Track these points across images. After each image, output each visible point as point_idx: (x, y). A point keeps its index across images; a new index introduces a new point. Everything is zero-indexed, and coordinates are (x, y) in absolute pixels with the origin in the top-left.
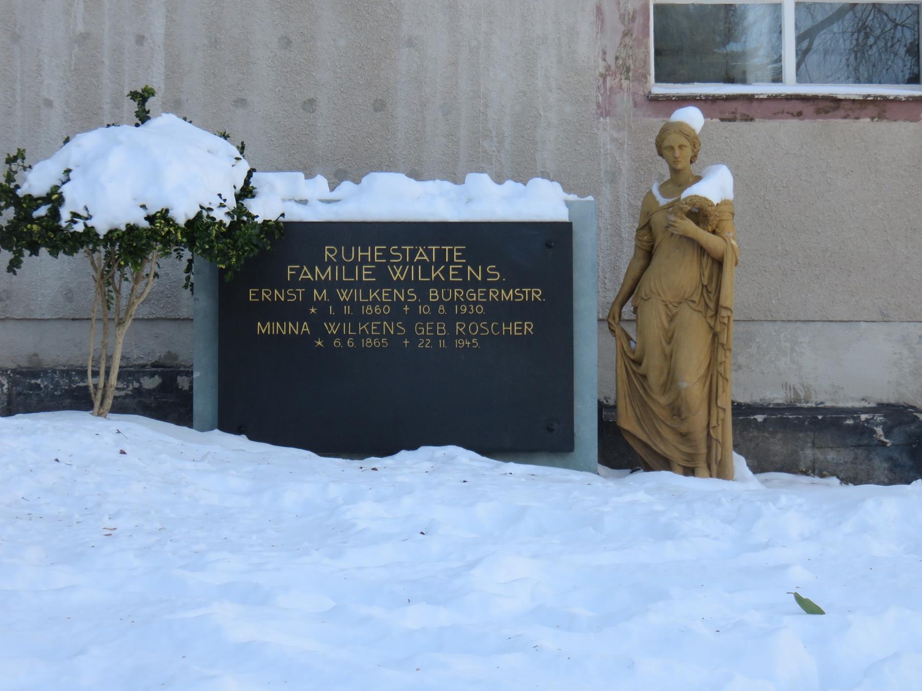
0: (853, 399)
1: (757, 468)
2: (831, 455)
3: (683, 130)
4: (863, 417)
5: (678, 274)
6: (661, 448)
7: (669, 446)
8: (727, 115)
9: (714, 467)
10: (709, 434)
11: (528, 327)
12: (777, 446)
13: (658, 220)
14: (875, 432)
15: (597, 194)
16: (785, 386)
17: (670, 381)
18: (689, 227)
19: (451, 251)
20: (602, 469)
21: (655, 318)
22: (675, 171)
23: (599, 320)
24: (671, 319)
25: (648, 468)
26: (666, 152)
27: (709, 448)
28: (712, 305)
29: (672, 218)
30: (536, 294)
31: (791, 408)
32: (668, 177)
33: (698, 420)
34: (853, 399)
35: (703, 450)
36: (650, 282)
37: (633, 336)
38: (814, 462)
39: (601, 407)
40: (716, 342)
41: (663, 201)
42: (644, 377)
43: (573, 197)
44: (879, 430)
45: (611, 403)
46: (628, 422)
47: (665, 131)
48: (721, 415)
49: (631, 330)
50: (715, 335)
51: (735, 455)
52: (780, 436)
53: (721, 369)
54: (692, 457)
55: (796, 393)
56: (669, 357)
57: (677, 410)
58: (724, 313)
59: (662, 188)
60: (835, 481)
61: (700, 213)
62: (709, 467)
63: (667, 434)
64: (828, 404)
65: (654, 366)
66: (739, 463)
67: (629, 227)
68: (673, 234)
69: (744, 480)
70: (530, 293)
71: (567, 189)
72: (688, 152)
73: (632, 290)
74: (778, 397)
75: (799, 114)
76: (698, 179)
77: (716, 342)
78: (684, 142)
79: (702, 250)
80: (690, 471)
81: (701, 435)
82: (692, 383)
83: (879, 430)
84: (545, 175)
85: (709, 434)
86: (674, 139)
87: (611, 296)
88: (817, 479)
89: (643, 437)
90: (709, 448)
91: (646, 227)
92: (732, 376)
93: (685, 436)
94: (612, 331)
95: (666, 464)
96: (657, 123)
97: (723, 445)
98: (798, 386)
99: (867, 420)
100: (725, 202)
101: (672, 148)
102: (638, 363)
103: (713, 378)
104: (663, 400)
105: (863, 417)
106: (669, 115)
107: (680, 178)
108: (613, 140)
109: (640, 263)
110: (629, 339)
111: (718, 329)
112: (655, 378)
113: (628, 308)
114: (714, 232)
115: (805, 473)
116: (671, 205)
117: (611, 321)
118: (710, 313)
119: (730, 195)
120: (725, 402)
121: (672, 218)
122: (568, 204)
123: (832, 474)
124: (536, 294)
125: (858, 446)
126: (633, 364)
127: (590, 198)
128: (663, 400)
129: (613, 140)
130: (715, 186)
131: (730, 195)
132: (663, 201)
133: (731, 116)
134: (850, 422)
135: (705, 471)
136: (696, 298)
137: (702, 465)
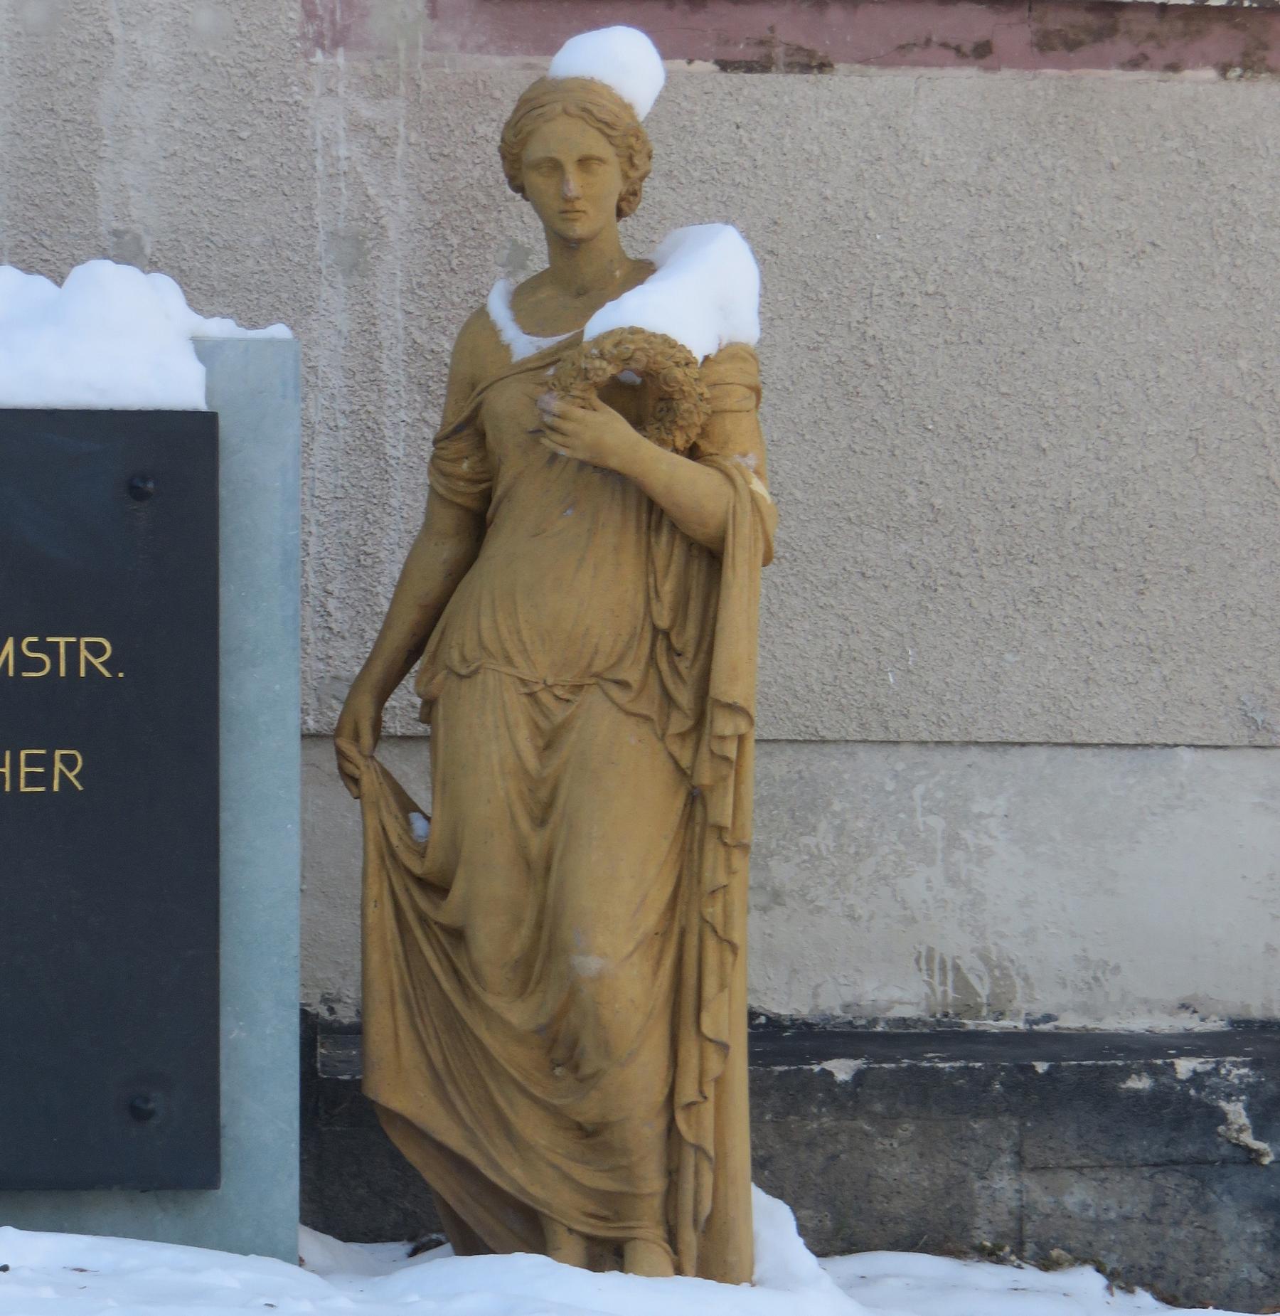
0: (1149, 1006)
1: (829, 1240)
2: (1078, 1195)
3: (592, 105)
4: (1184, 1067)
5: (570, 592)
6: (513, 1174)
7: (536, 1166)
8: (741, 51)
9: (689, 1238)
10: (671, 1129)
11: (67, 768)
12: (899, 1162)
13: (507, 405)
14: (1223, 1118)
15: (299, 311)
16: (928, 961)
17: (545, 949)
18: (612, 433)
20: (313, 1243)
21: (495, 736)
22: (565, 245)
23: (308, 737)
24: (549, 742)
25: (470, 1245)
26: (535, 180)
27: (673, 1174)
28: (684, 697)
29: (555, 404)
30: (94, 655)
31: (945, 1035)
32: (540, 261)
33: (638, 1081)
34: (1149, 1006)
35: (654, 1183)
36: (478, 620)
37: (421, 794)
38: (1021, 1215)
39: (313, 1030)
40: (698, 821)
41: (523, 345)
42: (458, 935)
43: (220, 328)
44: (1236, 1111)
45: (346, 1015)
46: (400, 1084)
47: (535, 106)
48: (714, 1065)
49: (411, 772)
50: (695, 798)
51: (760, 1200)
52: (907, 1128)
53: (714, 911)
54: (614, 1205)
55: (963, 984)
56: (541, 871)
57: (566, 1048)
58: (724, 725)
59: (520, 299)
60: (1088, 1280)
61: (647, 389)
62: (672, 1238)
63: (534, 1128)
64: (1070, 1022)
65: (489, 902)
66: (772, 1224)
67: (409, 428)
68: (560, 460)
69: (786, 1282)
70: (73, 650)
71: (201, 296)
72: (610, 181)
73: (417, 639)
74: (901, 996)
75: (982, 52)
76: (642, 271)
77: (698, 821)
78: (597, 145)
79: (653, 513)
80: (606, 1254)
81: (645, 1133)
82: (615, 956)
83: (1236, 1111)
84: (126, 250)
85: (671, 1129)
86: (563, 137)
87: (350, 658)
88: (1031, 1276)
89: (454, 1139)
90: (673, 1174)
91: (467, 432)
92: (749, 929)
93: (592, 1136)
94: (352, 781)
95: (529, 1230)
96: (506, 75)
97: (719, 1163)
98: (969, 962)
99: (1196, 1079)
100: (731, 353)
101: (555, 166)
102: (437, 887)
103: (687, 942)
104: (519, 1014)
105: (1184, 1067)
106: (552, 48)
107: (580, 269)
108: (358, 127)
109: (445, 551)
110: (407, 806)
111: (705, 776)
112: (494, 940)
113: (405, 698)
114: (693, 452)
115: (992, 1255)
116: (550, 359)
117: (346, 745)
118: (679, 723)
119: (748, 330)
120: (726, 1021)
121: (555, 404)
122: (205, 350)
123: (1082, 1258)
124: (94, 655)
125: (1167, 1164)
126: (421, 889)
127: (279, 331)
128: (519, 1014)
129: (358, 127)
130: (697, 295)
131: (748, 330)
132: (523, 345)
133: (753, 54)
134: (1140, 1083)
135: (660, 1254)
136: (633, 674)
137: (649, 1231)
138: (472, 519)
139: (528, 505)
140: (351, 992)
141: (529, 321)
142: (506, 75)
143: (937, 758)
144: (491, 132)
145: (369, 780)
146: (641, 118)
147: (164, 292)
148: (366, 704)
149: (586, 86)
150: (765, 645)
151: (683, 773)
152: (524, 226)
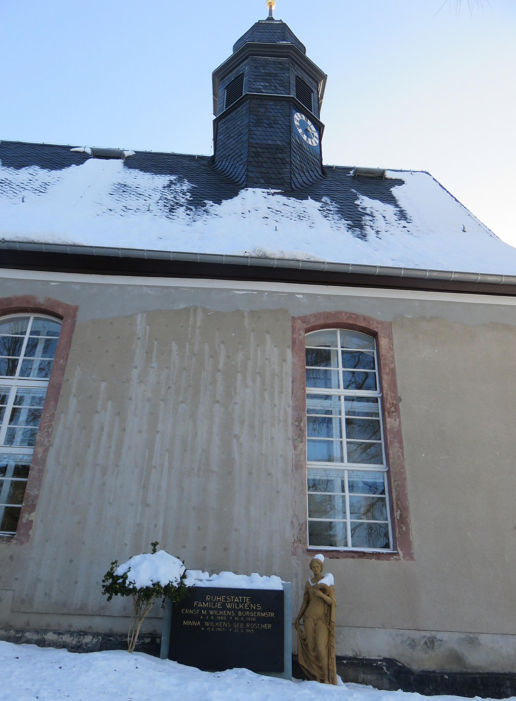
0: (375, 656)
1: (345, 681)
2: (369, 677)
3: (317, 561)
4: (379, 663)
5: (317, 610)
6: (313, 672)
7: (315, 671)
8: (331, 557)
9: (331, 680)
10: (328, 668)
11: (270, 626)
12: (351, 672)
13: (311, 591)
14: (383, 669)
15: (291, 581)
16: (353, 650)
17: (315, 647)
18: (321, 594)
19: (246, 599)
20: (293, 679)
21: (310, 624)
22: (316, 575)
23: (293, 624)
24: (315, 625)
25: (309, 680)
26: (313, 569)
27: (329, 673)
28: (328, 621)
29: (315, 590)
30: (272, 615)
31: (354, 658)
32: (313, 576)
33: (325, 661)
34: (375, 656)
35: (327, 673)
36: (309, 612)
37: (303, 630)
38: (364, 679)
39: (293, 655)
40: (330, 634)
41: (312, 584)
42: (307, 645)
43: (284, 582)
44: (385, 668)
45: (296, 653)
46: (302, 662)
47: (313, 561)
48: (332, 660)
49: (302, 628)
50: (330, 632)
51: (337, 675)
52: (351, 669)
53: (332, 644)
54: (323, 676)
55: (356, 653)
56: (315, 639)
57: (318, 658)
58: (332, 624)
59: (312, 580)
60: (371, 687)
61: (324, 589)
62: (329, 680)
63: (315, 667)
64: (367, 657)
65: (310, 641)
66: (339, 679)
67: (301, 593)
68: (315, 596)
69: (340, 685)
71: (282, 579)
72: (320, 569)
73: (303, 614)
74: (350, 654)
75: (353, 557)
76: (323, 577)
77: (330, 634)
78: (318, 565)
79: (325, 602)
80: (322, 681)
81: (326, 668)
82: (323, 651)
83: (385, 668)
84: (275, 574)
85: (328, 668)
86: (315, 564)
87: (296, 616)
88: (365, 686)
89: (307, 667)
90: (329, 673)
91: (307, 593)
92: (335, 646)
93: (321, 668)
94: (296, 628)
95: (314, 678)
96: (310, 558)
97: (333, 671)
98: (357, 651)
99: (380, 664)
100: (331, 586)
101: (315, 567)
102: (305, 640)
103: (329, 647)
104: (313, 654)
105: (379, 663)
106: (314, 556)
107: (317, 577)
108: (296, 563)
109: (305, 605)
110: (302, 631)
111: (330, 629)
112: (310, 646)
113: (301, 620)
114: (328, 596)
115: (361, 683)
116: (314, 586)
117: (296, 625)
118: (328, 623)
119: (333, 583)
120: (333, 656)
121: (315, 590)
122: (283, 584)
123: (370, 684)
124: (272, 615)
125: (378, 674)
126: (303, 640)
127: (289, 582)
128: (313, 654)
129: (296, 563)
130: (328, 580)
131: (333, 583)
132: (312, 584)
134: (375, 664)
135: (327, 682)
136: (323, 618)
137: (327, 679)
138: (307, 602)
139: (313, 601)
140: (296, 652)
141: (313, 582)
142: (310, 558)
143: (353, 628)
144: (309, 564)
145: (298, 629)
146: (323, 562)
147: (279, 579)
148: (298, 621)
149: (317, 559)
150: (335, 616)
151: (328, 629)
152: (312, 573)
